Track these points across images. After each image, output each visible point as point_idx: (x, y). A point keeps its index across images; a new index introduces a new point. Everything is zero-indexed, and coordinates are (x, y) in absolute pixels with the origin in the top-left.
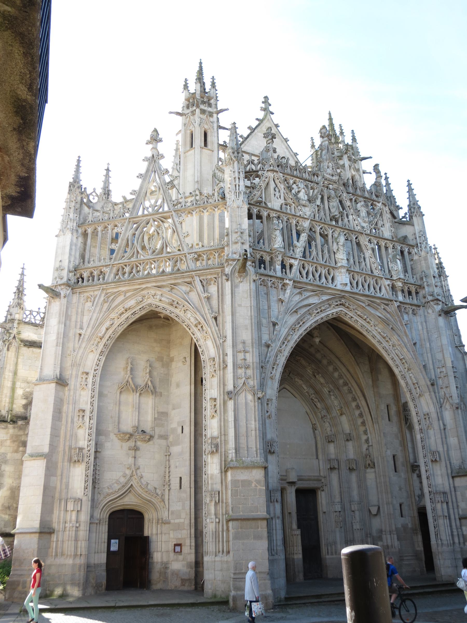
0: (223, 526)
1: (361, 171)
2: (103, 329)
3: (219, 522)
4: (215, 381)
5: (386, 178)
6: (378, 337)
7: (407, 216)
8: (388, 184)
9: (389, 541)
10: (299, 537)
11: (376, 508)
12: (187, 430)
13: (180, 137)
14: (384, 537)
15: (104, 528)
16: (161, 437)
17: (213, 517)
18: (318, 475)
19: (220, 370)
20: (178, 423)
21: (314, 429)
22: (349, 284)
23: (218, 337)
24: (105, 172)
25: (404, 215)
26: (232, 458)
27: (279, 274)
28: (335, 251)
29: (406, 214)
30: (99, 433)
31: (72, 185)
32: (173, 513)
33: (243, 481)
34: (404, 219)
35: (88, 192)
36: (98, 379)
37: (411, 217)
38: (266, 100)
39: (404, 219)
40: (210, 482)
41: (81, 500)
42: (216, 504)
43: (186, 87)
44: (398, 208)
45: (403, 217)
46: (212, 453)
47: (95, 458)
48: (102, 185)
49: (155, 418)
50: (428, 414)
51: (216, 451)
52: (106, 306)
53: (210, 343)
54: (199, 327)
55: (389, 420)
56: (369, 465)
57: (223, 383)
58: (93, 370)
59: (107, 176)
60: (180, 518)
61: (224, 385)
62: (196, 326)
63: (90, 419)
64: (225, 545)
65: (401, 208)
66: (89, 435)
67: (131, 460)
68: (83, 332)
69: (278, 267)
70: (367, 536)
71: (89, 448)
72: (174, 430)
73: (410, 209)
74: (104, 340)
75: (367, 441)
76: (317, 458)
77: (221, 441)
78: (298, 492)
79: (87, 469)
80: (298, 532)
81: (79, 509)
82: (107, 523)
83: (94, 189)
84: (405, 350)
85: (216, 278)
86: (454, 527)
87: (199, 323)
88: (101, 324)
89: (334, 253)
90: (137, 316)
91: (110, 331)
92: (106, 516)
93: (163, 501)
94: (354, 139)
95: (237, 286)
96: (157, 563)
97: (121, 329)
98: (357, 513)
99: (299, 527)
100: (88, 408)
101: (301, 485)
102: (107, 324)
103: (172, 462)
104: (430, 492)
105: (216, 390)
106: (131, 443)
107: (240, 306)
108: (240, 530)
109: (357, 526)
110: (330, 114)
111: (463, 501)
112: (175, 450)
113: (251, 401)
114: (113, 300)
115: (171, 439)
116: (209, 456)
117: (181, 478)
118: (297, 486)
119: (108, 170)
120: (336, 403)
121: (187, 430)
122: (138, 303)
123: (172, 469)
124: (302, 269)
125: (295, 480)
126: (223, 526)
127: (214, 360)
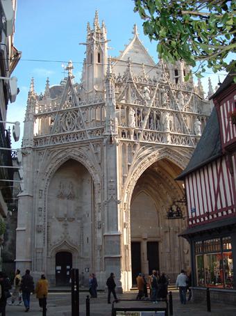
2: (48, 168)
10: (148, 265)
12: (90, 215)
15: (54, 260)
16: (78, 219)
21: (158, 212)
22: (170, 141)
24: (46, 83)
27: (132, 140)
30: (49, 217)
36: (47, 193)
47: (48, 229)
52: (49, 158)
53: (97, 175)
69: (132, 136)
72: (84, 216)
76: (159, 226)
78: (148, 243)
79: (44, 234)
80: (147, 262)
88: (47, 167)
90: (63, 162)
92: (54, 255)
97: (56, 169)
99: (148, 259)
101: (149, 240)
102: (50, 167)
106: (63, 222)
109: (177, 259)
112: (85, 225)
114: (52, 154)
115: (83, 219)
119: (48, 81)
121: (90, 215)
122: (63, 156)
125: (146, 237)
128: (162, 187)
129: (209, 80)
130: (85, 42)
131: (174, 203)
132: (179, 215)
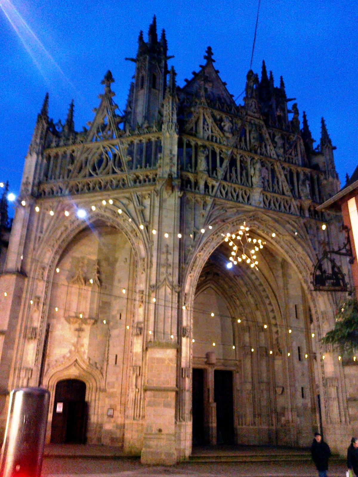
0: (141, 396)
1: (286, 111)
2: (59, 233)
3: (138, 392)
4: (144, 276)
5: (304, 116)
6: (286, 247)
7: (320, 148)
8: (305, 122)
9: (290, 417)
11: (281, 389)
13: (134, 81)
14: (286, 413)
17: (134, 387)
18: (234, 358)
19: (147, 268)
20: (118, 311)
23: (148, 242)
24: (69, 107)
25: (316, 147)
26: (151, 339)
28: (252, 175)
29: (318, 146)
31: (40, 116)
32: (108, 383)
33: (158, 359)
34: (317, 151)
35: (54, 122)
37: (322, 149)
38: (209, 50)
39: (317, 151)
40: (134, 359)
41: (32, 371)
42: (137, 378)
43: (141, 38)
44: (313, 141)
45: (316, 149)
46: (137, 335)
48: (66, 117)
49: (99, 306)
50: (326, 313)
51: (140, 333)
54: (134, 233)
55: (297, 317)
56: (277, 353)
57: (148, 279)
58: (49, 266)
59: (72, 111)
60: (114, 388)
61: (150, 280)
62: (131, 232)
63: (44, 305)
64: (141, 410)
65: (315, 141)
66: (42, 318)
67: (75, 339)
68: (42, 236)
70: (272, 412)
71: (41, 328)
73: (322, 142)
74: (59, 242)
75: (277, 332)
77: (144, 325)
78: (216, 372)
81: (30, 376)
82: (55, 389)
83: (60, 121)
84: (308, 259)
85: (149, 194)
86: (342, 408)
87: (134, 230)
89: (252, 177)
91: (64, 236)
93: (102, 374)
94: (282, 84)
95: (165, 200)
96: (94, 423)
98: (265, 392)
100: (43, 296)
103: (111, 342)
104: (323, 378)
105: (144, 285)
107: (166, 217)
108: (152, 398)
110: (264, 62)
111: (351, 386)
113: (170, 294)
116: (135, 338)
117: (116, 356)
118: (215, 368)
120: (252, 301)
123: (111, 348)
124: (222, 190)
126: (141, 396)
127: (144, 260)
128: (241, 282)
129: (323, 121)
130: (134, 57)
131: (325, 254)
132: (338, 284)
